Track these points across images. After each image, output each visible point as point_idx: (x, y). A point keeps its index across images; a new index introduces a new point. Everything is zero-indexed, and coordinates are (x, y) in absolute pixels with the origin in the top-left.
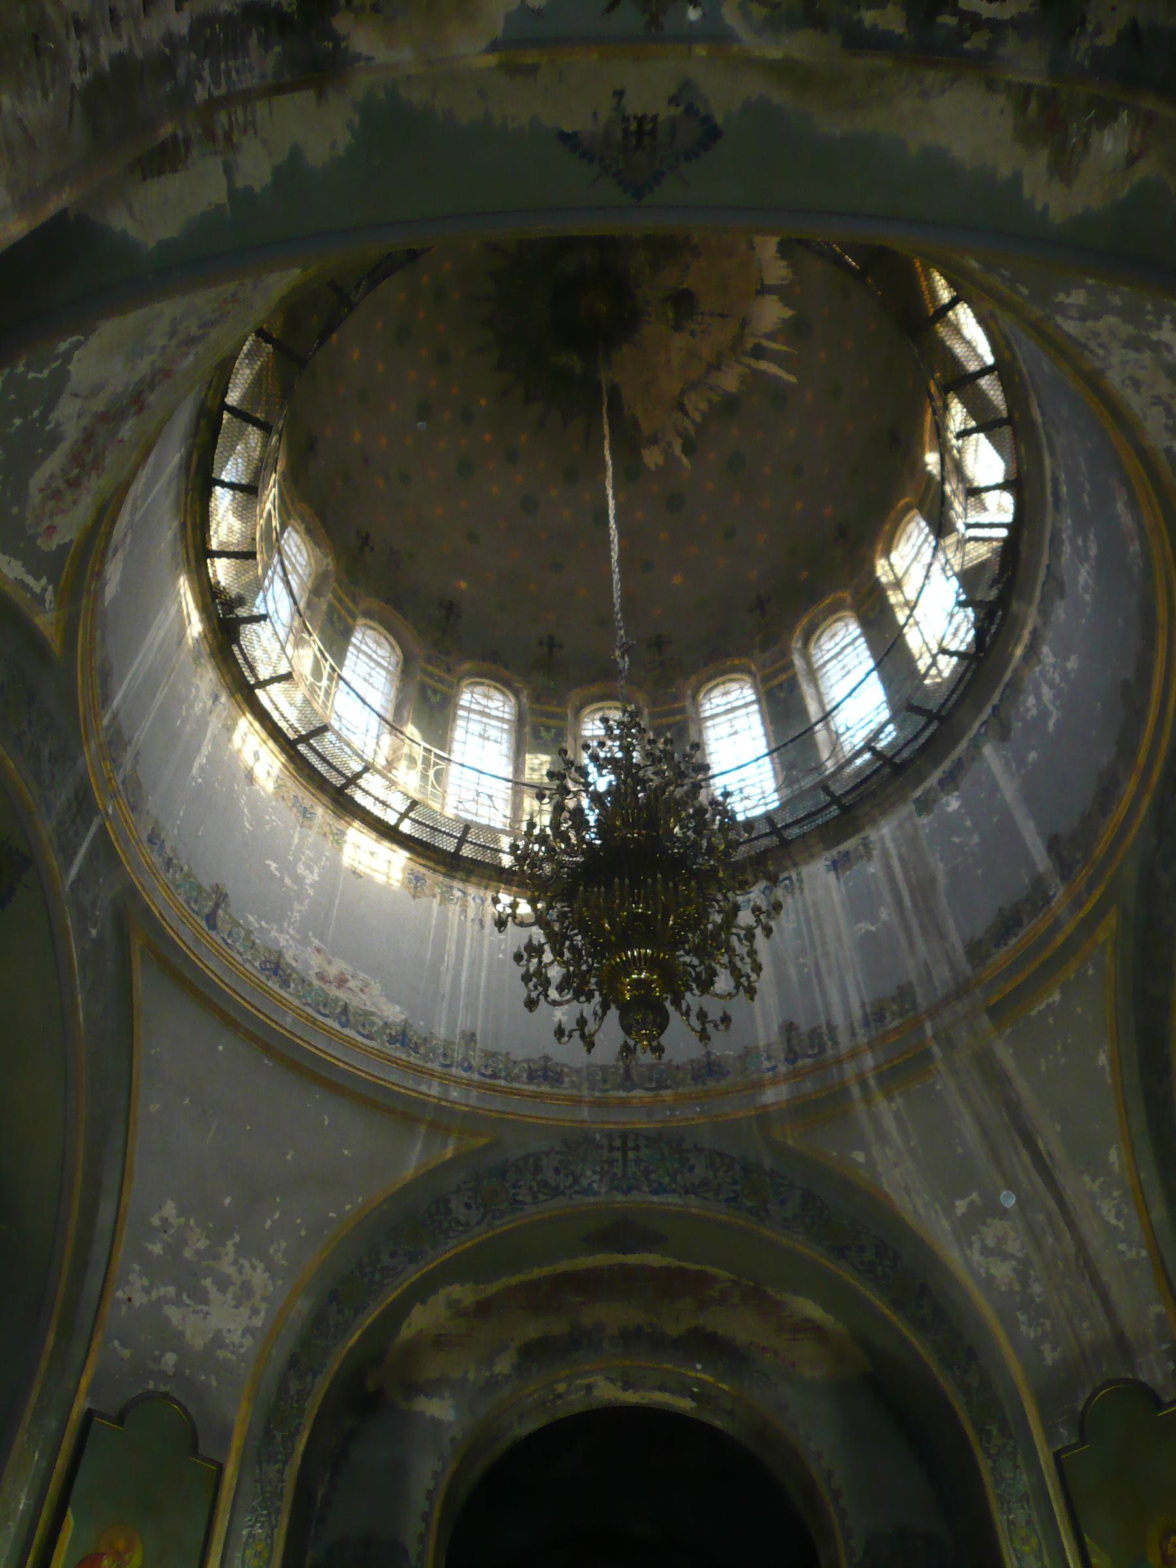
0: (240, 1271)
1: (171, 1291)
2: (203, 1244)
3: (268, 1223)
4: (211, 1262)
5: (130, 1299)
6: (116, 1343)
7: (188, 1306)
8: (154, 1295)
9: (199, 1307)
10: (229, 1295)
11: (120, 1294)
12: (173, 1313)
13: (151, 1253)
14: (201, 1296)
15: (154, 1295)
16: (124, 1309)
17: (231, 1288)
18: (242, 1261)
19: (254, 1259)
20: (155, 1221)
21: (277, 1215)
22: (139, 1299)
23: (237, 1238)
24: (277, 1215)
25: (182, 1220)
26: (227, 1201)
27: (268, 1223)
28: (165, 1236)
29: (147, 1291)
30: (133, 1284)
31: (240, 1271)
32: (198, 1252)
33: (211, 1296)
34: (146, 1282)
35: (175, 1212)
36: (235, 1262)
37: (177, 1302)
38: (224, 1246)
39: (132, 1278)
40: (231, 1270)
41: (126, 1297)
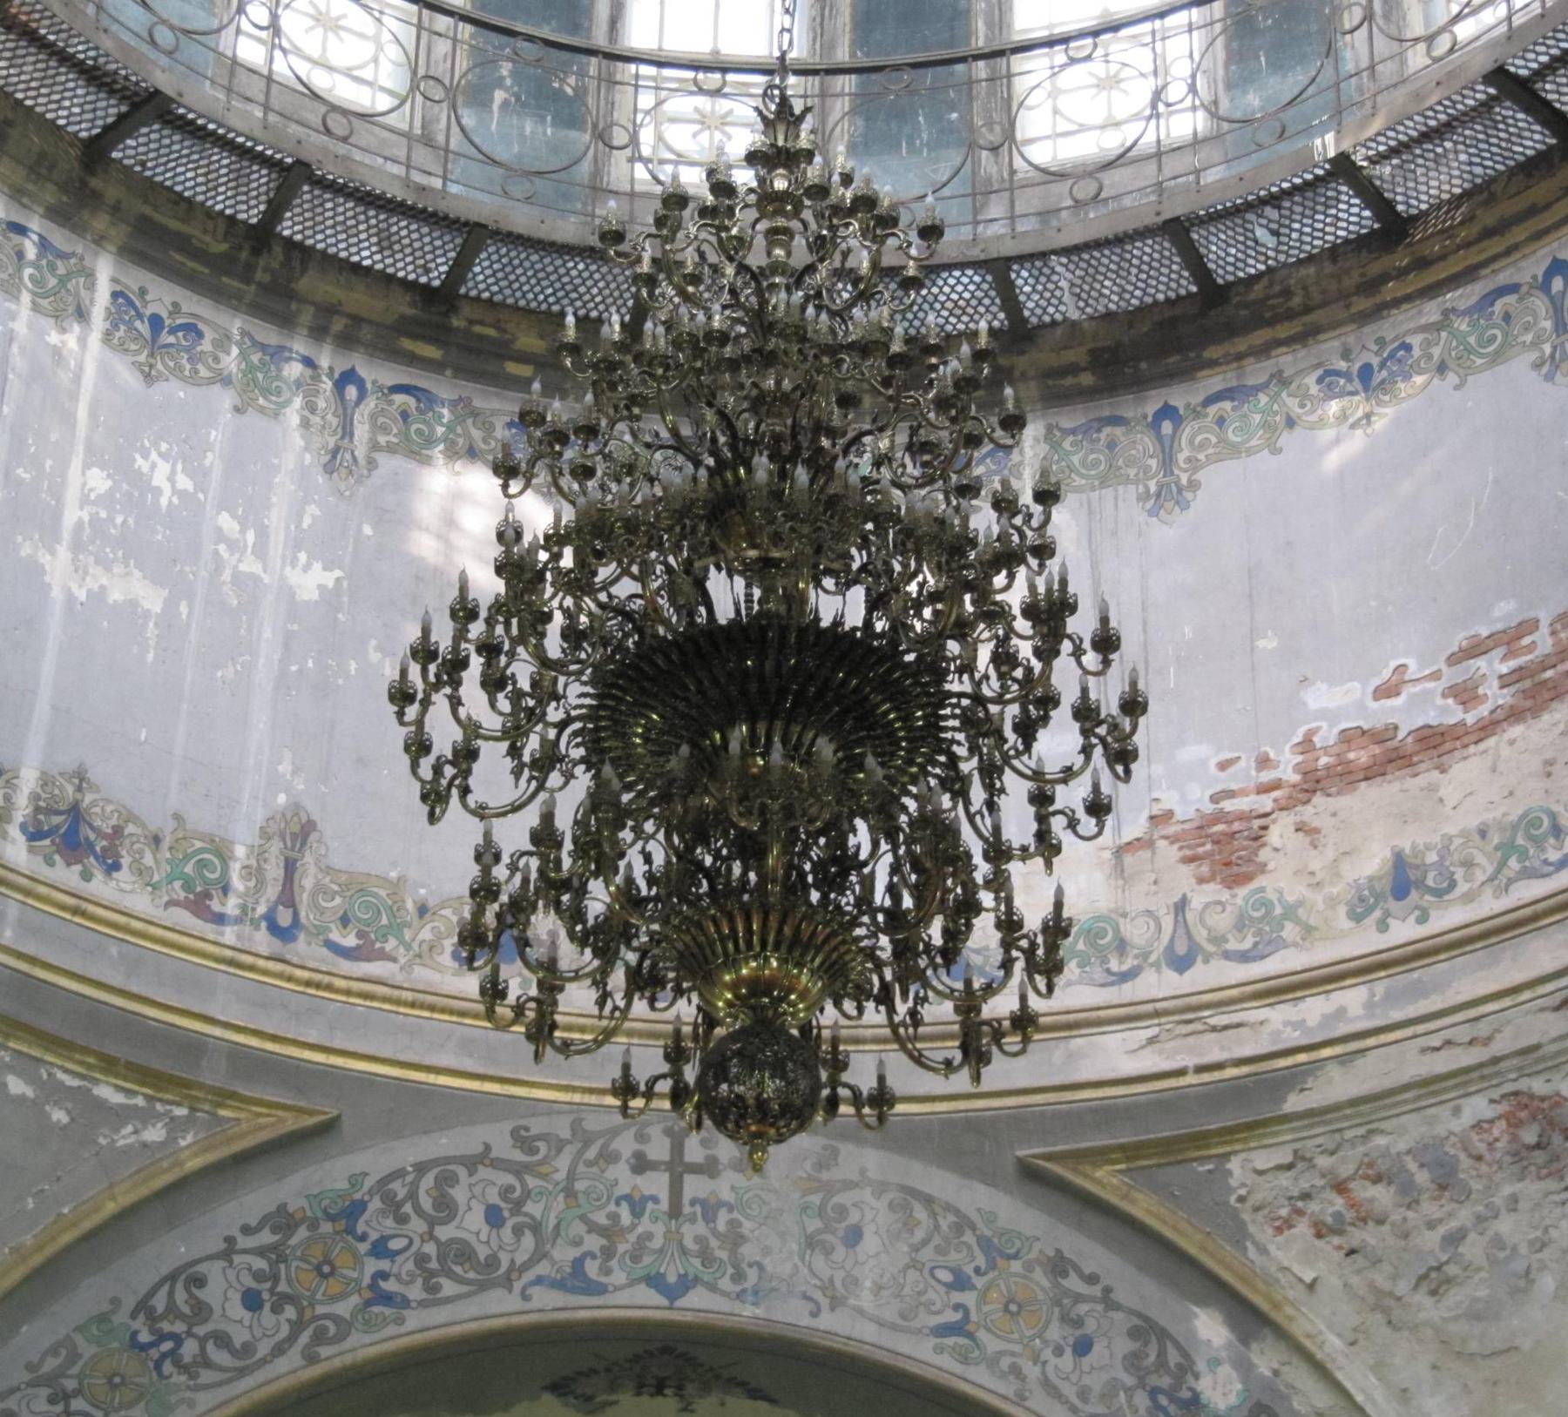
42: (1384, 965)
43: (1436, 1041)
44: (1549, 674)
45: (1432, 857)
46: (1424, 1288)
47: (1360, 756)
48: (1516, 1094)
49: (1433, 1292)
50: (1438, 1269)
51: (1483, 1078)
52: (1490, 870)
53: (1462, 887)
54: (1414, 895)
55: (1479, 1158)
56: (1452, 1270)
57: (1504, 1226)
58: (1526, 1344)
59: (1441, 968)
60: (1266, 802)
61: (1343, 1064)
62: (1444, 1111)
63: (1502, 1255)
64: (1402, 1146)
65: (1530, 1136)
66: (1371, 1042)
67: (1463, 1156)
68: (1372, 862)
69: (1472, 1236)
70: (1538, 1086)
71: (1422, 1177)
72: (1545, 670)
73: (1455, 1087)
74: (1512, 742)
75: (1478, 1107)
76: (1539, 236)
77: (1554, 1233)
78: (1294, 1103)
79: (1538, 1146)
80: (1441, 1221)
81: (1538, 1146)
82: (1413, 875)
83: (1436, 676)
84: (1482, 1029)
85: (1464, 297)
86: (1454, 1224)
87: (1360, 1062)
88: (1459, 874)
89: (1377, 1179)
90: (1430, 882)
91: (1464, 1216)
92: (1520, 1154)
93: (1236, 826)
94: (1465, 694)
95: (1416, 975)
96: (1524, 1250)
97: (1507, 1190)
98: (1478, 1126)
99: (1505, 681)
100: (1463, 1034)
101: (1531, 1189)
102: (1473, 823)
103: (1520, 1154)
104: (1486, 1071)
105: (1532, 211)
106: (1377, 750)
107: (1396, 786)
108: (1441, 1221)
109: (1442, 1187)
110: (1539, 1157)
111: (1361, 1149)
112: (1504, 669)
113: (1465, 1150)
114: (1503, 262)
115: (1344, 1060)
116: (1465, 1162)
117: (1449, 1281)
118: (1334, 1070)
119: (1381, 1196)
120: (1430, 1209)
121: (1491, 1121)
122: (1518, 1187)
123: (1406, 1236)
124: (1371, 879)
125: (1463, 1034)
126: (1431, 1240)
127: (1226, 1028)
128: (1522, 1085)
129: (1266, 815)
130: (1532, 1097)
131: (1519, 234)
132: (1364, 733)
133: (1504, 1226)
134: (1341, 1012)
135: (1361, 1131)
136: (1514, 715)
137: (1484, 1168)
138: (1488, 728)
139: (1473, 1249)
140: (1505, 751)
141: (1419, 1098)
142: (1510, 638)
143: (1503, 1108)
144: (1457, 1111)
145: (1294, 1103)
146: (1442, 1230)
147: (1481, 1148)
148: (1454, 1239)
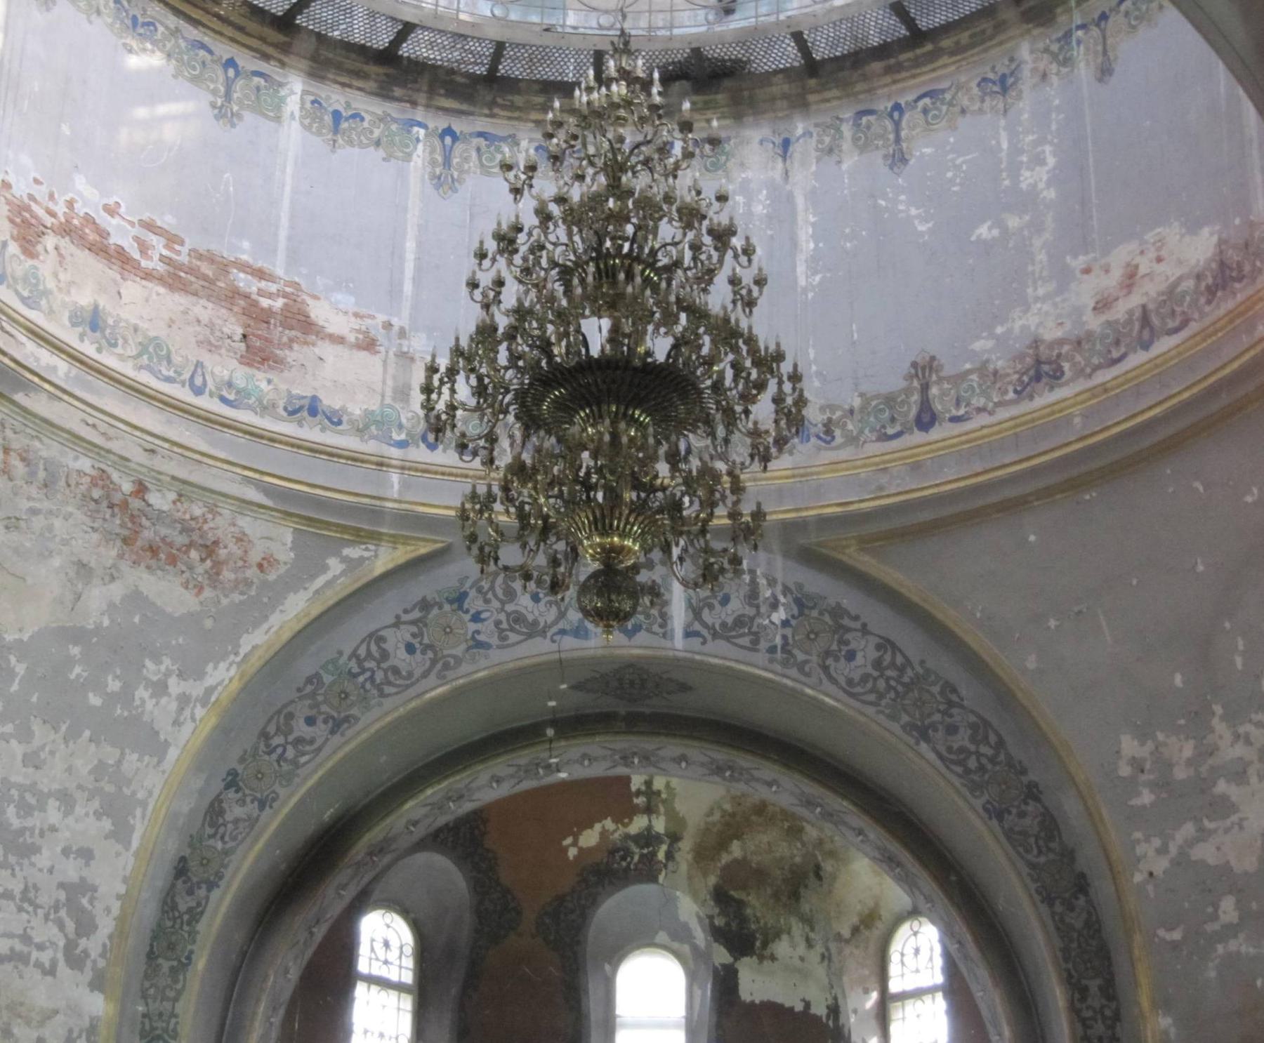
0: (1248, 742)
1: (1188, 829)
2: (1188, 750)
3: (1239, 661)
4: (1210, 761)
5: (1151, 874)
6: (1161, 932)
7: (1215, 831)
8: (1173, 849)
9: (1228, 822)
10: (1254, 780)
11: (1138, 878)
12: (1205, 853)
13: (1144, 807)
14: (1223, 807)
15: (1173, 849)
16: (1150, 888)
17: (1252, 771)
18: (1241, 730)
19: (1253, 716)
20: (1125, 770)
21: (1241, 644)
22: (1160, 865)
23: (1218, 709)
24: (1241, 644)
25: (1150, 745)
26: (1178, 680)
27: (1239, 661)
28: (1144, 778)
29: (1163, 850)
30: (1145, 856)
31: (1248, 742)
32: (1189, 762)
33: (1234, 798)
34: (1157, 842)
35: (1136, 743)
36: (1237, 737)
37: (1203, 835)
38: (1212, 731)
39: (1139, 850)
40: (1239, 750)
41: (1146, 875)
42: (82, 362)
43: (91, 421)
44: (182, 274)
45: (110, 321)
46: (5, 522)
47: (92, 236)
48: (103, 471)
49: (7, 528)
50: (18, 519)
51: (98, 454)
52: (134, 353)
53: (119, 350)
54: (98, 334)
55: (69, 486)
56: (22, 524)
57: (58, 523)
58: (30, 581)
59: (100, 384)
60: (49, 221)
61: (50, 398)
62: (71, 454)
63: (47, 535)
64: (44, 454)
65: (96, 494)
66: (66, 397)
67: (63, 479)
68: (84, 298)
69: (41, 517)
70: (115, 476)
71: (42, 474)
72: (181, 270)
73: (85, 448)
74: (158, 294)
75: (85, 464)
76: (233, 40)
77: (74, 542)
78: (19, 397)
79: (96, 501)
80: (34, 499)
81: (96, 501)
82: (100, 323)
83: (132, 224)
84: (111, 432)
85: (194, 33)
86: (38, 505)
87: (56, 403)
88: (120, 342)
89: (23, 459)
90: (108, 331)
91: (46, 505)
92: (87, 497)
93: (33, 221)
94: (144, 248)
95: (90, 378)
96: (57, 539)
97: (70, 509)
98: (79, 472)
99: (162, 258)
100: (103, 427)
101: (79, 516)
102: (133, 321)
103: (87, 497)
104: (102, 453)
105: (241, 29)
106: (98, 238)
107: (101, 266)
108: (34, 499)
109: (46, 486)
110: (92, 505)
111: (27, 441)
112: (165, 252)
113: (67, 477)
114: (212, 34)
115: (52, 396)
116: (62, 483)
117: (17, 528)
118: (44, 396)
119: (19, 468)
120: (33, 491)
121: (85, 474)
122: (75, 511)
123: (16, 494)
124: (82, 307)
125: (103, 427)
126: (25, 505)
127: (7, 332)
128: (110, 470)
129: (46, 227)
130: (109, 477)
131: (229, 31)
132: (94, 223)
133: (58, 523)
134: (55, 369)
135: (34, 433)
136: (161, 280)
137: (67, 491)
138: (148, 275)
139: (38, 522)
140: (154, 297)
141: (67, 440)
142: (172, 240)
143: (94, 473)
144: (76, 458)
145: (19, 397)
146: (31, 504)
147: (73, 483)
148: (34, 512)
